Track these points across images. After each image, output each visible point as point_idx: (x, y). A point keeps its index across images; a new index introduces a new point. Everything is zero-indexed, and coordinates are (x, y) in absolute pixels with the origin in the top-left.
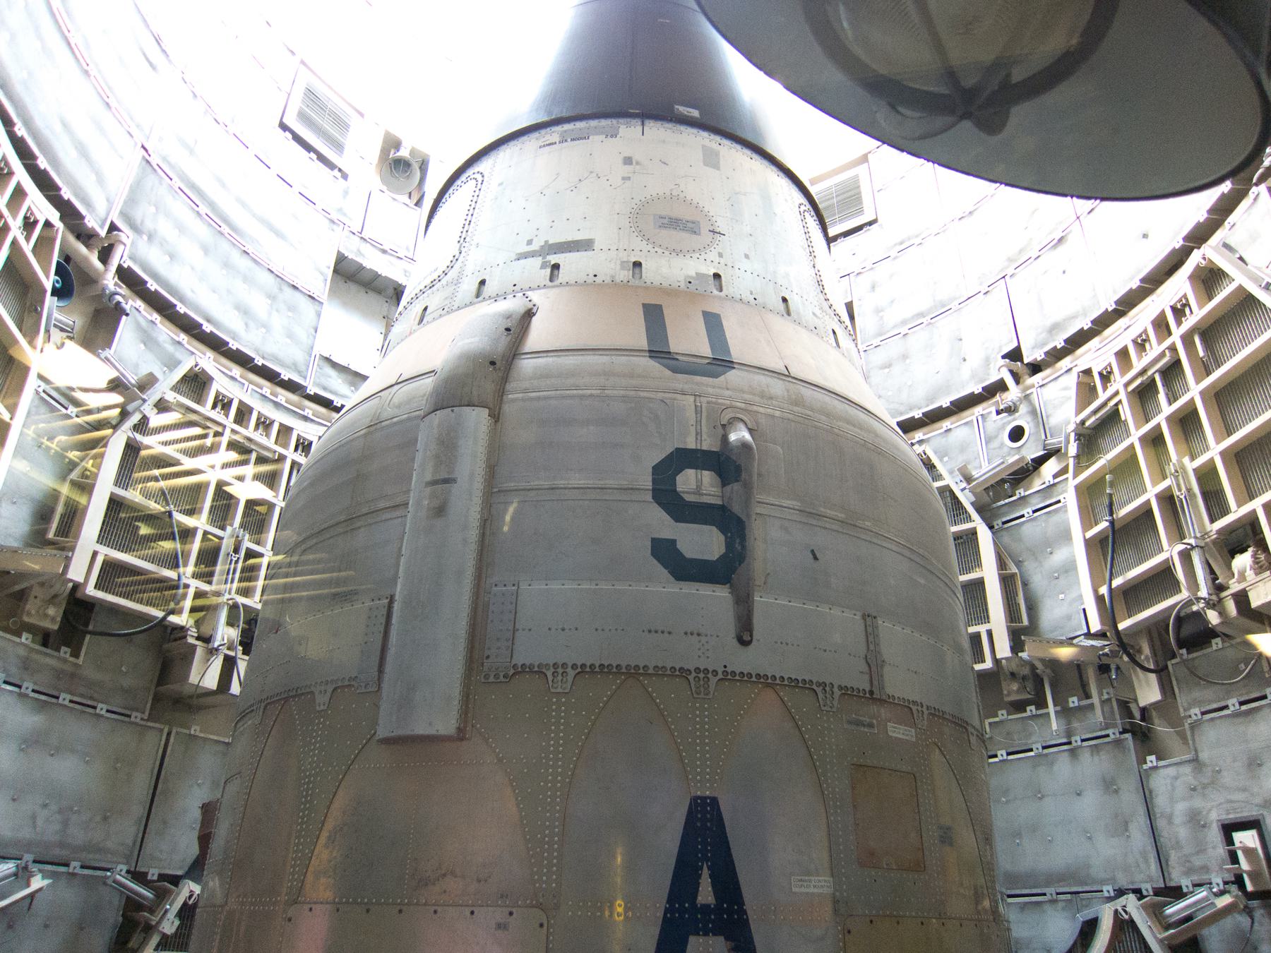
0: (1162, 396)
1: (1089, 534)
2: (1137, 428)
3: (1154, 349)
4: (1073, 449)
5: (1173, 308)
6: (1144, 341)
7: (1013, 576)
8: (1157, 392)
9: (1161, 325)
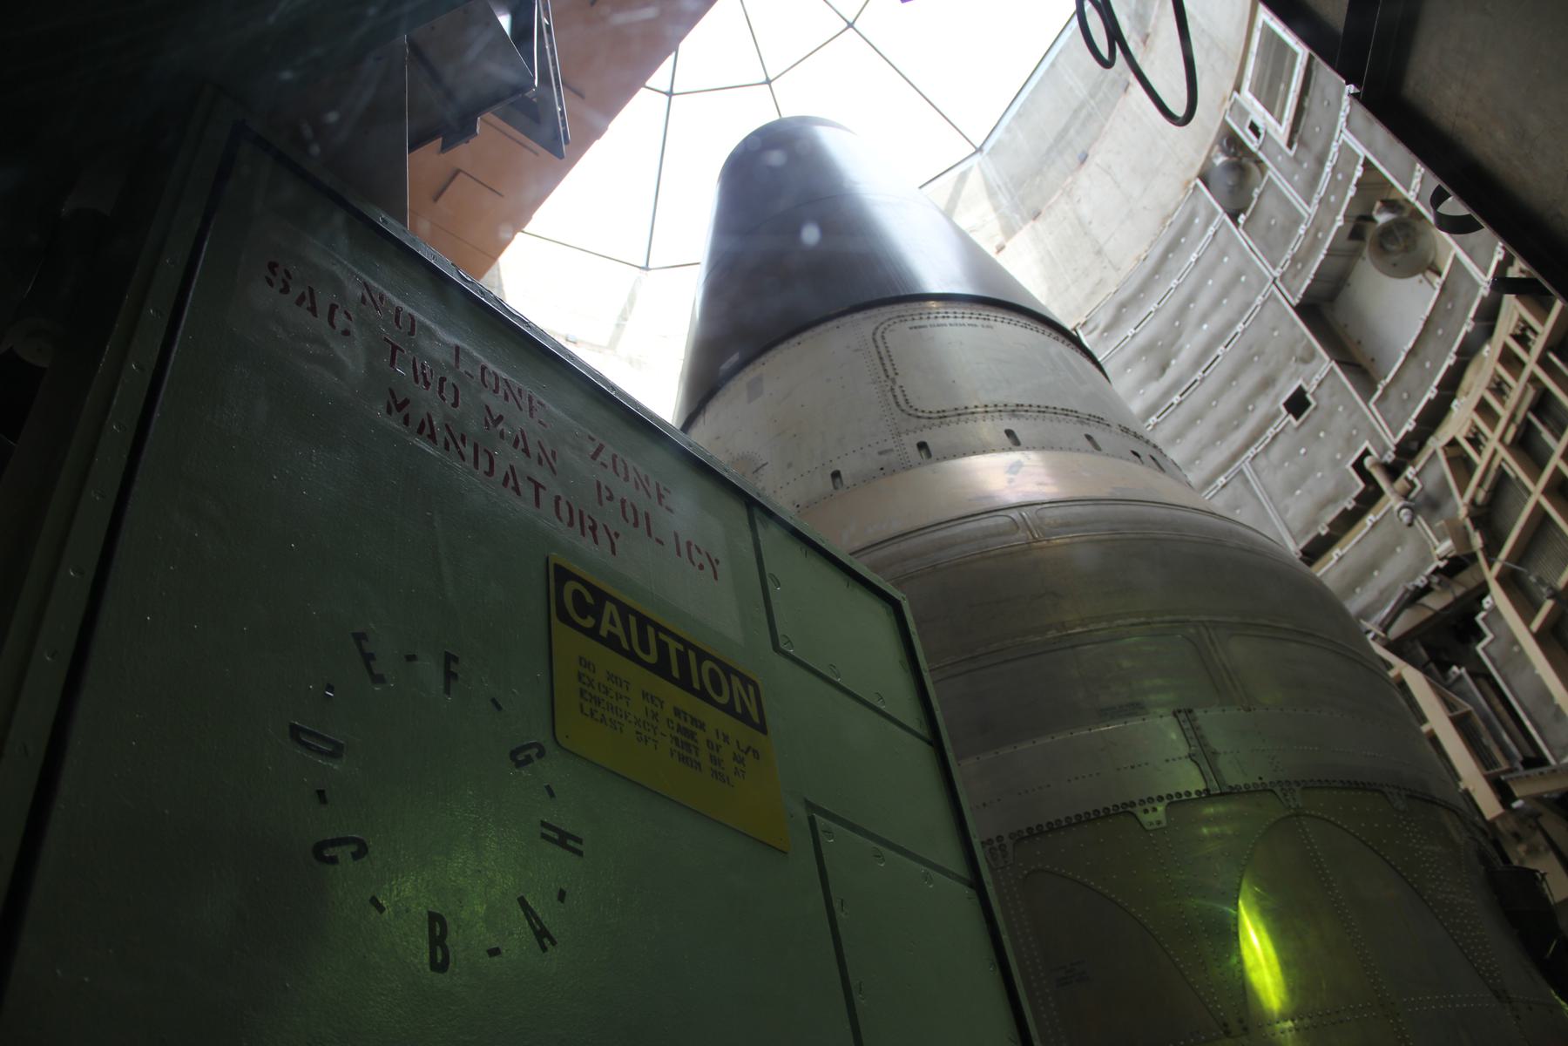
0: (1547, 436)
1: (1536, 625)
2: (1535, 481)
3: (1517, 387)
4: (1477, 541)
5: (1514, 337)
6: (1499, 384)
7: (1467, 715)
8: (1539, 433)
9: (1509, 360)
